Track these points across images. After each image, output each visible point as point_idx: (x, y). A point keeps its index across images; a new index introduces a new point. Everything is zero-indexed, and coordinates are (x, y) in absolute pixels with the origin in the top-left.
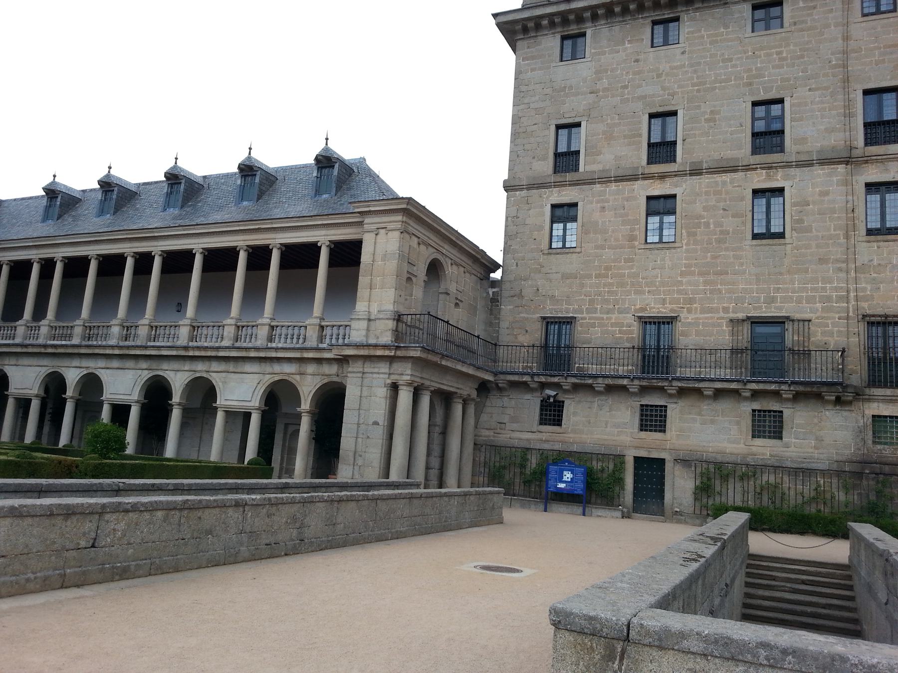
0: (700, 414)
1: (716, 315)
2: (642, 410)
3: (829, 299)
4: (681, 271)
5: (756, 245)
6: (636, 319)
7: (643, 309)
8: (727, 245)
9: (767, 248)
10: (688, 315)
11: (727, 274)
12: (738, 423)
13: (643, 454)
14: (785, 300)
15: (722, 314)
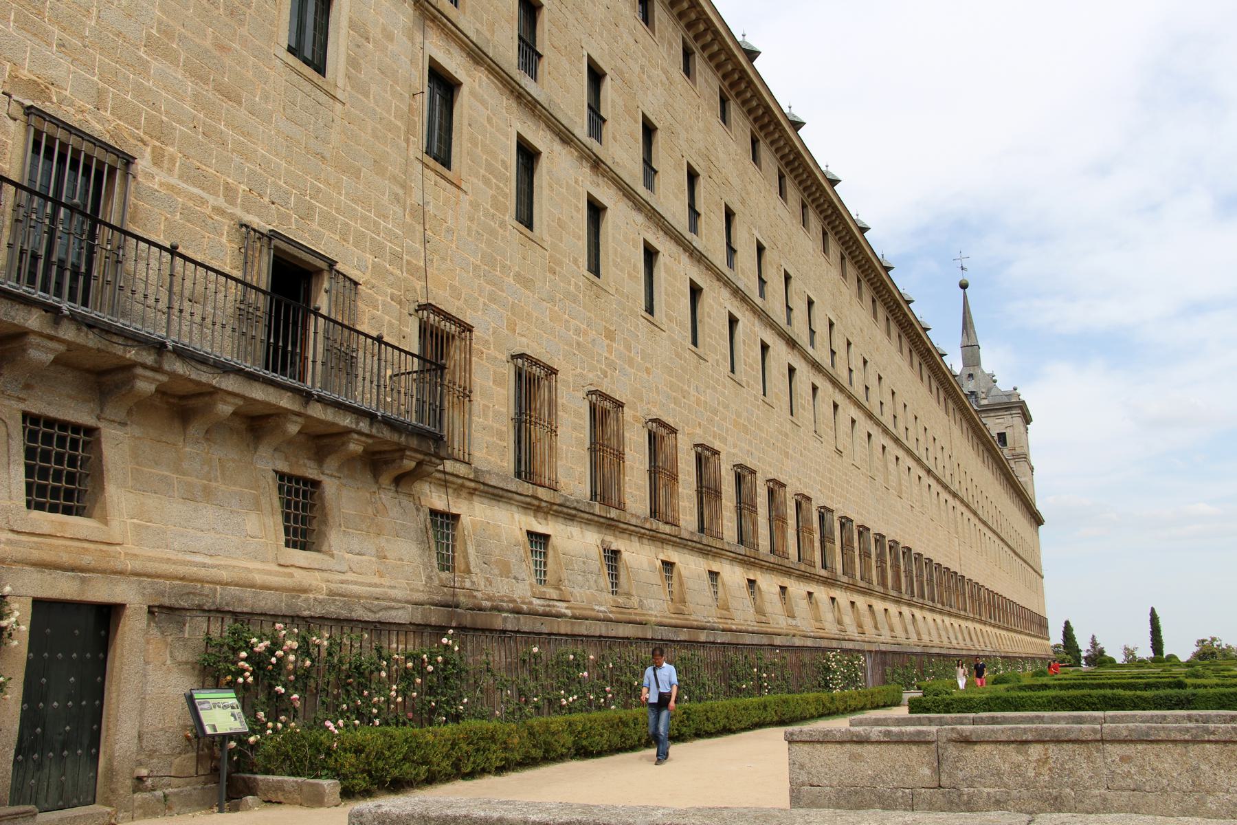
0: (178, 470)
1: (212, 200)
2: (31, 436)
3: (378, 250)
4: (149, 36)
5: (293, 69)
6: (19, 113)
7: (41, 90)
8: (244, 31)
9: (308, 87)
10: (154, 170)
11: (239, 103)
12: (257, 506)
13: (63, 588)
14: (328, 221)
15: (221, 202)
